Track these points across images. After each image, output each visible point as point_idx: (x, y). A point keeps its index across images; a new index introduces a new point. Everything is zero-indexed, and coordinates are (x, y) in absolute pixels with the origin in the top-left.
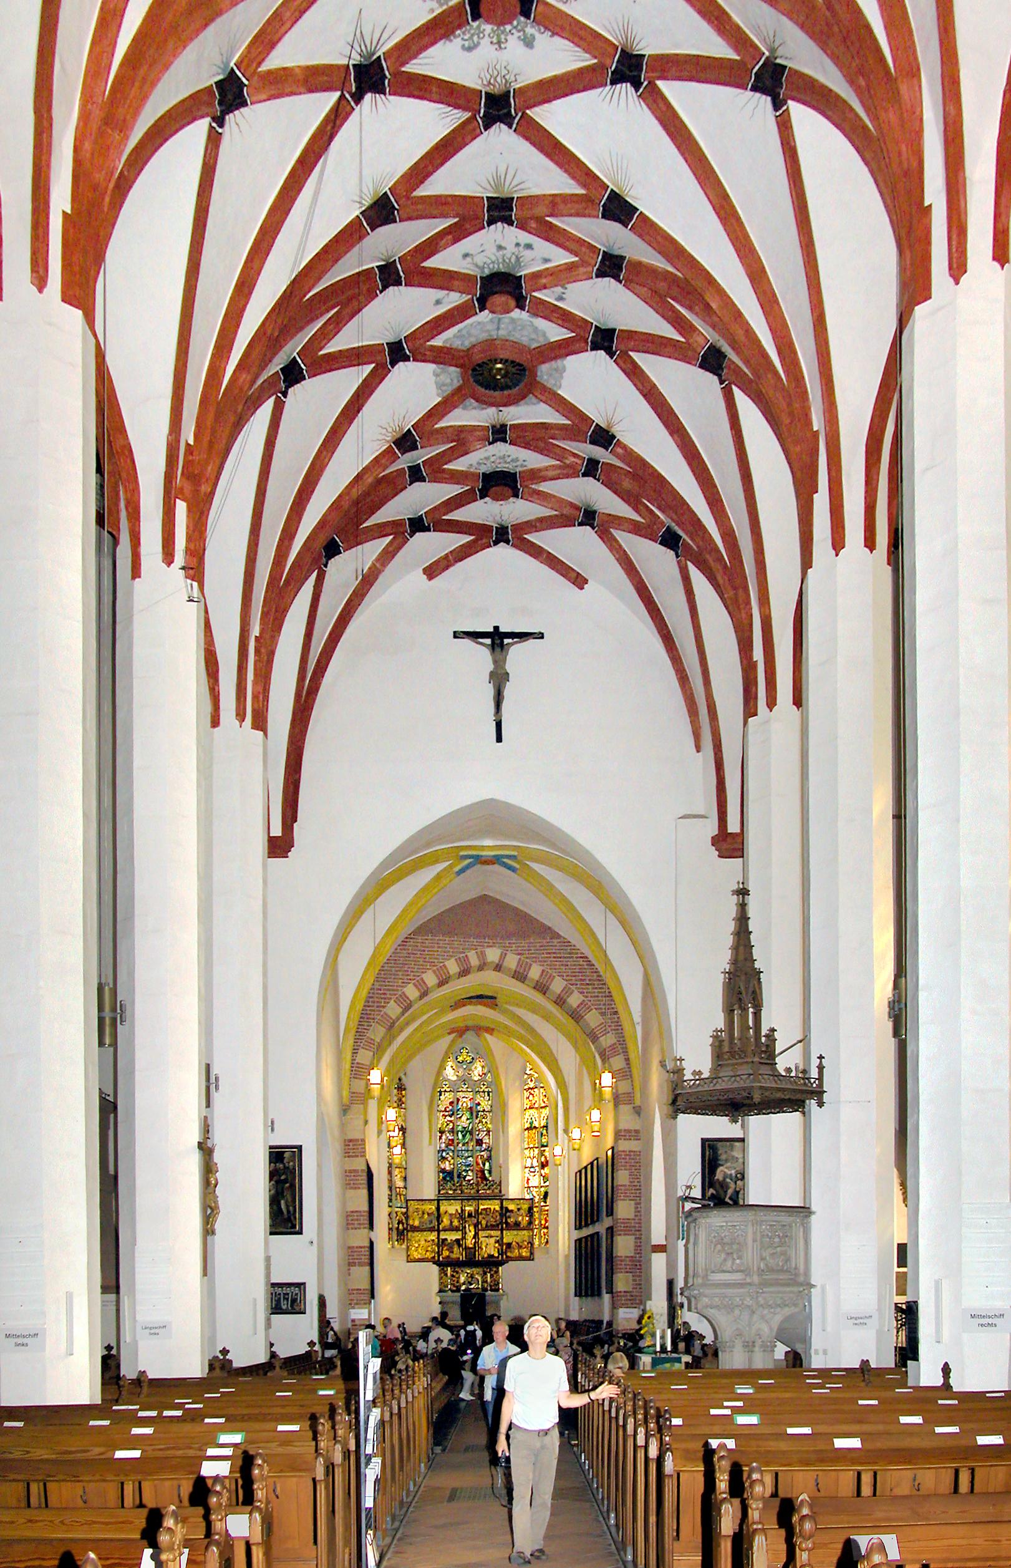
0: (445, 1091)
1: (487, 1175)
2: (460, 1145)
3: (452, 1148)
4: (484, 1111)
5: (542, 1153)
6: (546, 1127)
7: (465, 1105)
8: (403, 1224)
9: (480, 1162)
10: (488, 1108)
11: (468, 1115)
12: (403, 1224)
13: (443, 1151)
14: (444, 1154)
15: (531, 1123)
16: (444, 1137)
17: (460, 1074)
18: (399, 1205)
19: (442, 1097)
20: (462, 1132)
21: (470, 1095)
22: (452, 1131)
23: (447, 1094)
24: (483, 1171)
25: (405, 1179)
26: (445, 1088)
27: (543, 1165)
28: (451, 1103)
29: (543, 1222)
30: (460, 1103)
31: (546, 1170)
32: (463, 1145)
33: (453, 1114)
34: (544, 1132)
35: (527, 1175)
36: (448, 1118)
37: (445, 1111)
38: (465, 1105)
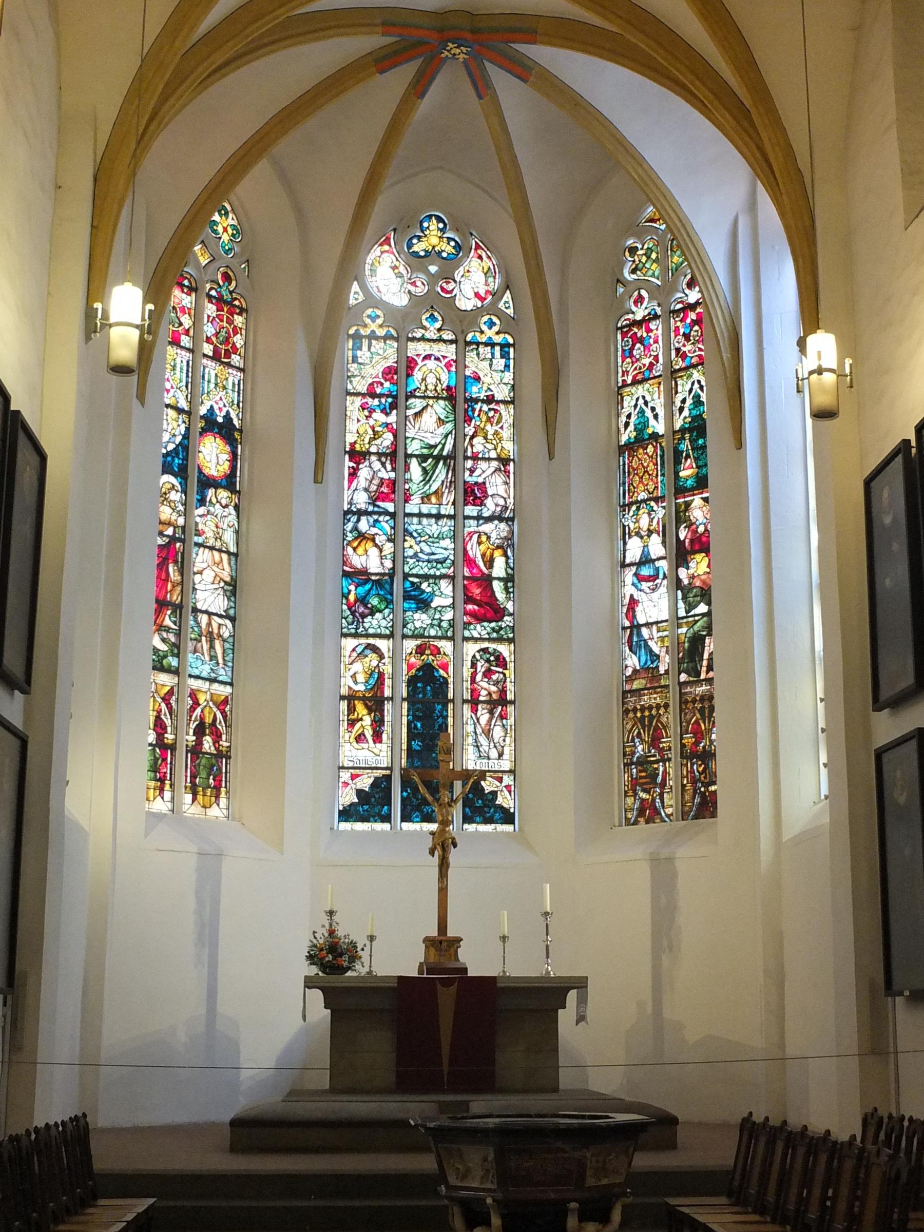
0: (373, 336)
1: (500, 595)
2: (416, 499)
3: (390, 507)
4: (490, 400)
5: (681, 516)
6: (697, 427)
7: (431, 380)
8: (217, 737)
9: (475, 551)
10: (502, 393)
11: (440, 408)
12: (217, 737)
13: (360, 513)
14: (363, 525)
15: (641, 427)
16: (364, 473)
17: (421, 289)
18: (205, 670)
19: (363, 355)
20: (423, 458)
21: (450, 351)
22: (392, 455)
23: (377, 346)
24: (486, 581)
25: (232, 589)
26: (373, 326)
27: (681, 556)
28: (389, 373)
29: (689, 739)
30: (418, 375)
31: (699, 565)
32: (426, 498)
33: (393, 406)
34: (685, 446)
35: (629, 590)
36: (379, 416)
37: (372, 394)
38: (431, 380)
